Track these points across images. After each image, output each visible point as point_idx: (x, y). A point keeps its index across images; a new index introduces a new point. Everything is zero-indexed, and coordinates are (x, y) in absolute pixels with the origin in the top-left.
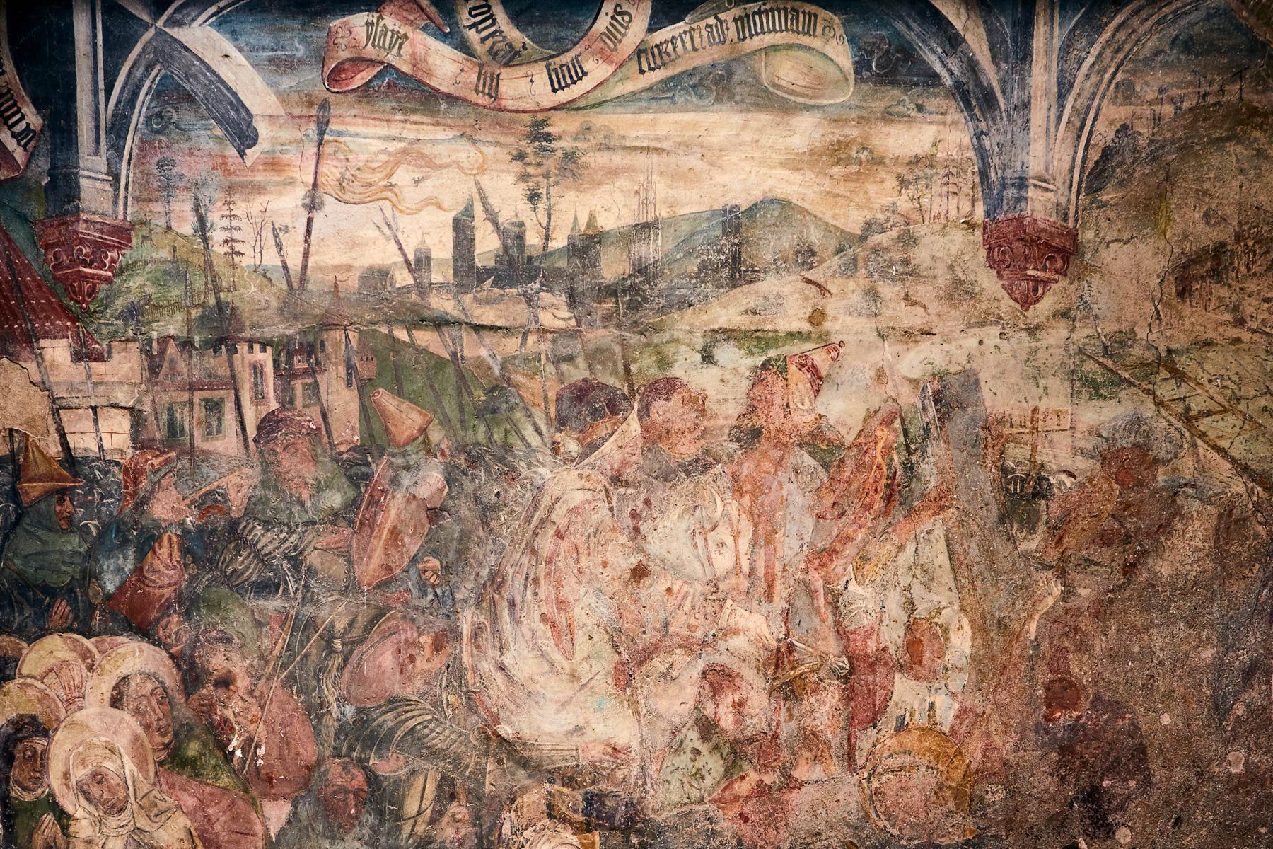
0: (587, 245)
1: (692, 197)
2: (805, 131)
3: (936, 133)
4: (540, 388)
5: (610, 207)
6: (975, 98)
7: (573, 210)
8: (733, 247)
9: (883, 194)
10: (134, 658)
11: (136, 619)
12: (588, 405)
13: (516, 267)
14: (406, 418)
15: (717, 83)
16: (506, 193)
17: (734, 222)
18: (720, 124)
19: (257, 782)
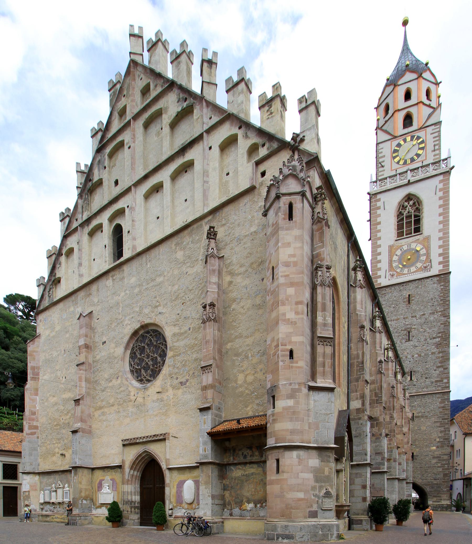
1: (251, 472)
3: (260, 469)
4: (245, 480)
5: (247, 473)
6: (262, 467)
8: (252, 474)
9: (259, 471)
10: (229, 492)
11: (229, 490)
12: (246, 481)
13: (244, 475)
14: (239, 482)
15: (252, 468)
17: (252, 473)
18: (252, 469)
19: (233, 497)
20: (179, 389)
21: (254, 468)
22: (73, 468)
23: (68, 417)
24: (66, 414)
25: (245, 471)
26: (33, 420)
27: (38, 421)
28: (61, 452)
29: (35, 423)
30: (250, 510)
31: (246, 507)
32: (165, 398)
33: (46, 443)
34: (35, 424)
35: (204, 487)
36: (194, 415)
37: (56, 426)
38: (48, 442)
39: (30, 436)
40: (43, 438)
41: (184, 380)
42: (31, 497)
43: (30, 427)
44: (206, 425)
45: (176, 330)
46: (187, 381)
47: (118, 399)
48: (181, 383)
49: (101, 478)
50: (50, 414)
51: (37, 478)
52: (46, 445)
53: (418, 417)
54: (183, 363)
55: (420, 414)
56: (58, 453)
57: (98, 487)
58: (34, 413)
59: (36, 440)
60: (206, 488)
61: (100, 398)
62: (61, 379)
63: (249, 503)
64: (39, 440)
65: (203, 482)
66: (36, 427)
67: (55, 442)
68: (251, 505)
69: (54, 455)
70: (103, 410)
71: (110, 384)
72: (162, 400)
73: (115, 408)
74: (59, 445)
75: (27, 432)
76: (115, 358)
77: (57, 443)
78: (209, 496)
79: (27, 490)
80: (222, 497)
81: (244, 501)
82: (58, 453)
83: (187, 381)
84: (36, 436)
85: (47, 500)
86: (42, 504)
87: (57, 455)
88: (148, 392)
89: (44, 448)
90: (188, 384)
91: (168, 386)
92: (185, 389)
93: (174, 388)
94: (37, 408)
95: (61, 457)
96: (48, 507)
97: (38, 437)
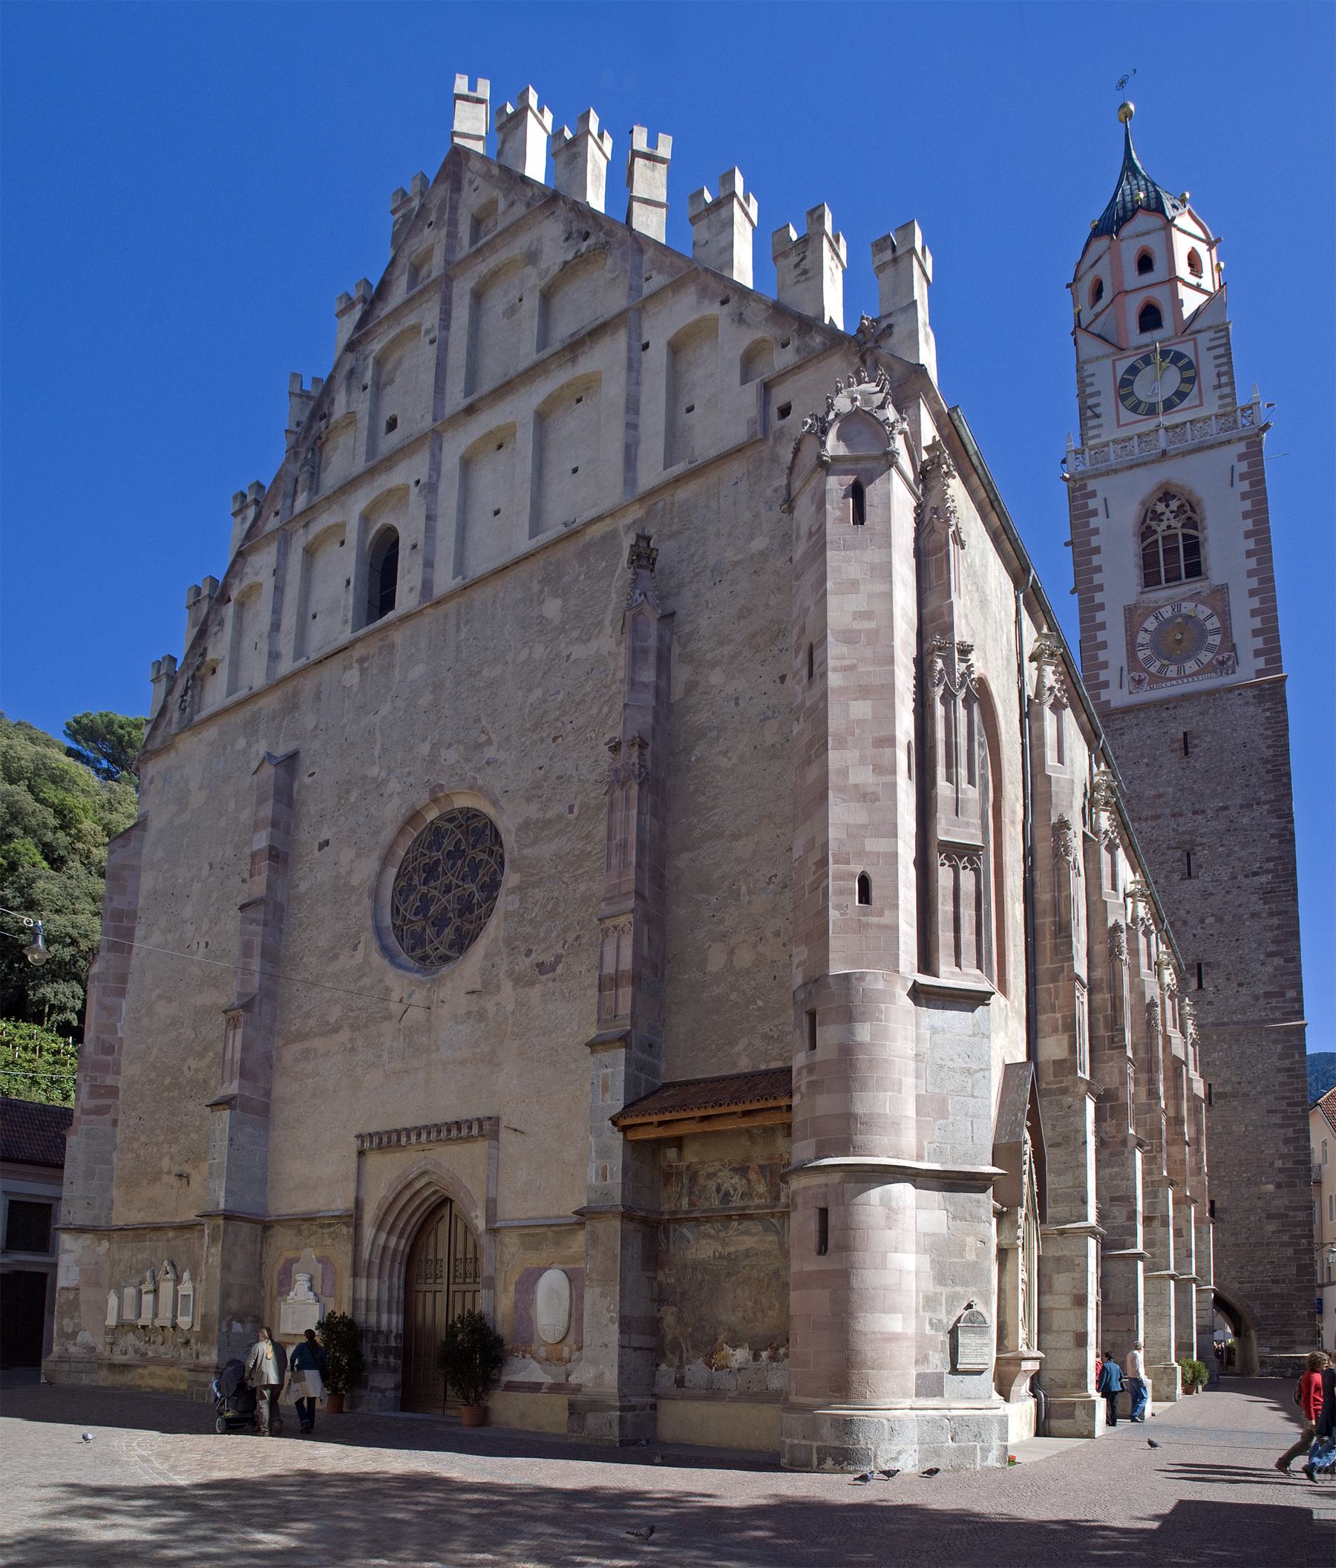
0: (729, 1254)
1: (742, 1248)
2: (756, 1238)
3: (772, 1238)
5: (732, 1249)
7: (728, 1250)
8: (747, 1254)
10: (674, 1309)
11: (674, 1304)
13: (721, 1257)
14: (707, 1278)
16: (720, 1248)
18: (745, 1238)
20: (532, 984)
21: (752, 1235)
24: (201, 1055)
25: (725, 1243)
26: (104, 1068)
27: (118, 1073)
28: (176, 1169)
29: (109, 1081)
30: (739, 1370)
31: (725, 1357)
32: (491, 1010)
33: (137, 1140)
35: (598, 1290)
36: (573, 1066)
38: (143, 1139)
39: (93, 1117)
40: (128, 1126)
41: (548, 958)
42: (83, 1308)
44: (608, 1095)
45: (532, 811)
46: (558, 959)
47: (352, 1010)
48: (541, 968)
49: (290, 1254)
52: (135, 1145)
53: (1222, 1096)
54: (549, 908)
55: (1228, 1088)
56: (169, 1172)
57: (281, 1283)
60: (603, 1295)
63: (735, 1347)
64: (118, 1130)
65: (594, 1276)
68: (740, 1356)
69: (156, 1177)
70: (306, 1044)
71: (333, 968)
72: (481, 1016)
73: (344, 1035)
74: (174, 1149)
75: (86, 1106)
76: (353, 889)
78: (612, 1320)
79: (72, 1284)
80: (654, 1326)
81: (721, 1338)
82: (169, 1172)
83: (558, 959)
84: (108, 1117)
87: (166, 1178)
88: (445, 992)
90: (559, 969)
91: (502, 976)
92: (550, 984)
93: (518, 981)
96: (130, 1340)
97: (115, 1123)
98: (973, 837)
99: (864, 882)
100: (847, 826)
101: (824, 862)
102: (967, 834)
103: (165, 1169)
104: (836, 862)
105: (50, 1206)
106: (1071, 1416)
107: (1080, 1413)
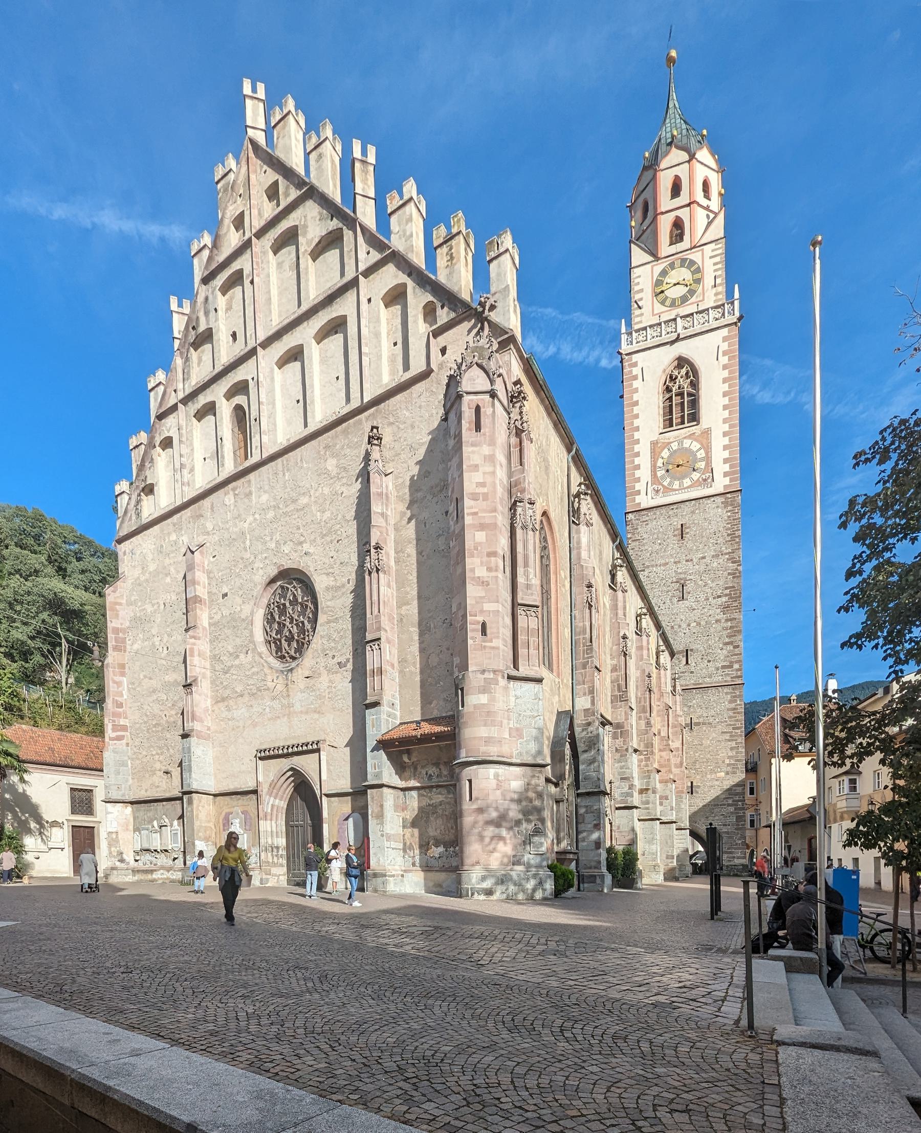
22: (185, 793)
23: (173, 712)
28: (164, 768)
34: (122, 723)
37: (155, 726)
38: (144, 753)
42: (121, 842)
43: (115, 728)
45: (330, 581)
50: (145, 707)
51: (129, 809)
58: (120, 705)
59: (125, 747)
61: (222, 683)
62: (161, 649)
66: (124, 728)
67: (154, 753)
77: (158, 754)
79: (114, 830)
82: (160, 770)
84: (124, 742)
85: (146, 846)
86: (136, 853)
89: (138, 762)
94: (125, 697)
95: (165, 776)
96: (148, 857)
98: (535, 600)
99: (484, 626)
100: (475, 598)
101: (465, 616)
102: (534, 598)
103: (158, 768)
104: (471, 615)
105: (92, 791)
106: (594, 882)
107: (598, 881)
